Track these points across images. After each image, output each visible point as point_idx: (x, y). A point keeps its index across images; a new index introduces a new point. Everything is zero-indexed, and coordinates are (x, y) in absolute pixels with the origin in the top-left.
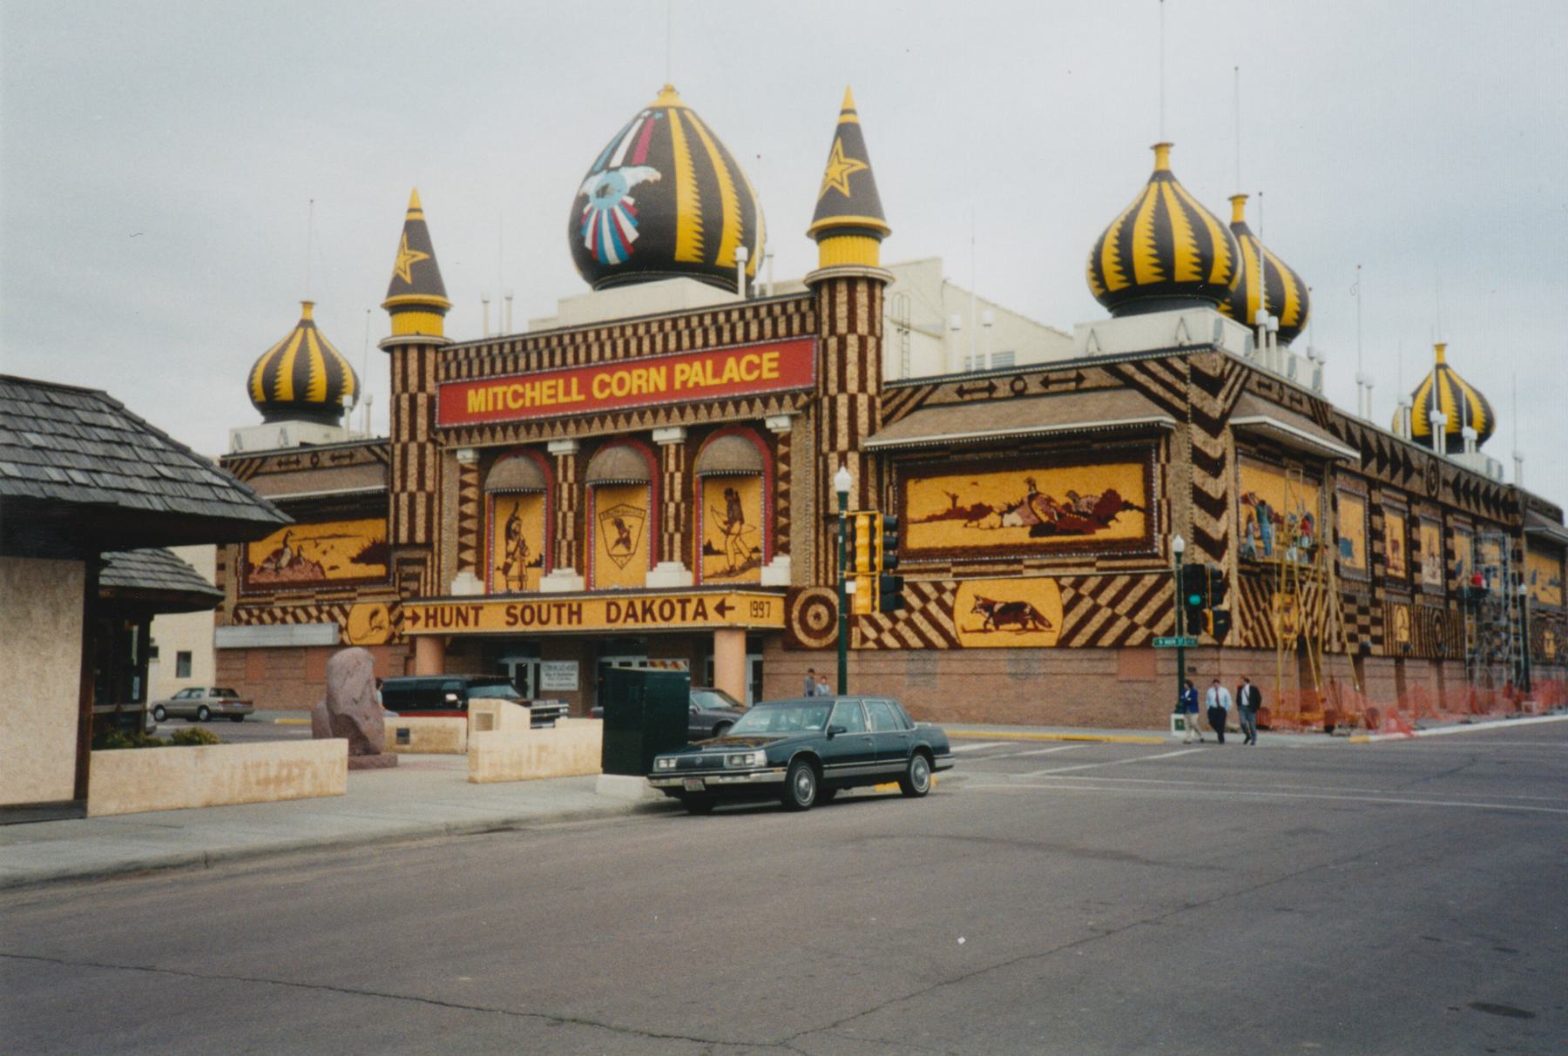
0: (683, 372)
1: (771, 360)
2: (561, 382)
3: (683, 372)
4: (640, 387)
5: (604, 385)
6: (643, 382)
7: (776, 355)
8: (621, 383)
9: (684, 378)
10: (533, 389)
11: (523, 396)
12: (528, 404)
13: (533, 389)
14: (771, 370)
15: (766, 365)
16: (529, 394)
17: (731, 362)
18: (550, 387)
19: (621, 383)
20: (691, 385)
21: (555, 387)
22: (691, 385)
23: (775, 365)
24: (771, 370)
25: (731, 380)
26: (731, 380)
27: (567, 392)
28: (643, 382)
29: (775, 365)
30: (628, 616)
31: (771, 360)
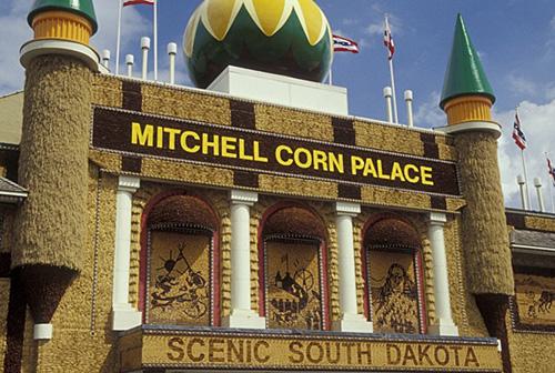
0: (358, 163)
1: (426, 172)
2: (242, 141)
3: (358, 163)
4: (320, 165)
5: (285, 156)
6: (323, 161)
7: (430, 169)
8: (303, 158)
9: (360, 167)
10: (210, 140)
11: (200, 143)
12: (205, 151)
13: (210, 140)
14: (427, 179)
15: (424, 175)
16: (206, 144)
17: (396, 165)
18: (228, 143)
19: (303, 158)
20: (365, 174)
21: (237, 144)
22: (365, 174)
23: (430, 176)
24: (427, 179)
25: (398, 178)
26: (398, 178)
27: (249, 151)
28: (323, 161)
29: (430, 176)
30: (406, 357)
31: (426, 172)
